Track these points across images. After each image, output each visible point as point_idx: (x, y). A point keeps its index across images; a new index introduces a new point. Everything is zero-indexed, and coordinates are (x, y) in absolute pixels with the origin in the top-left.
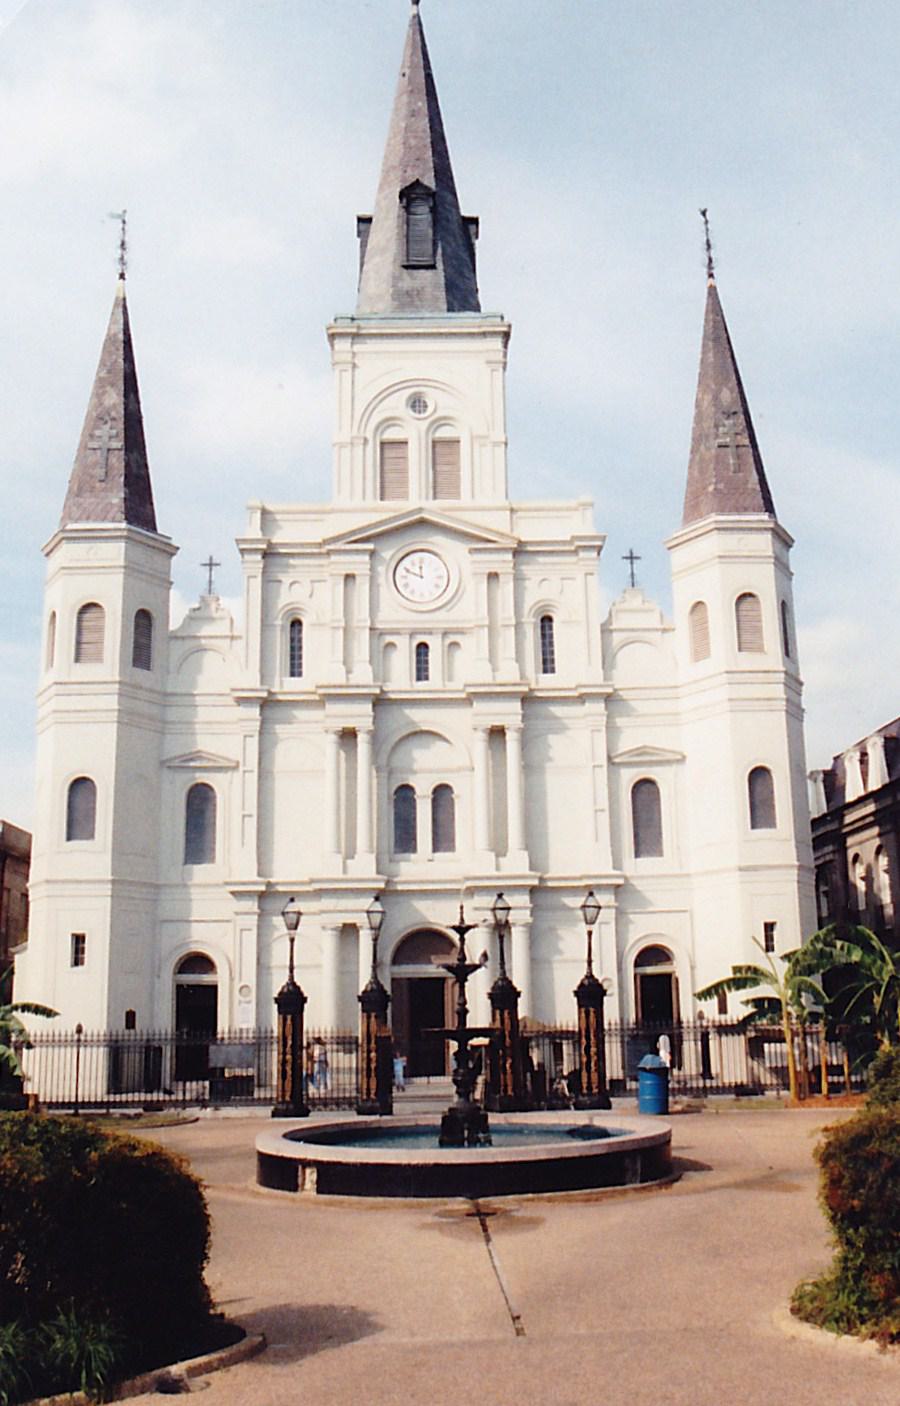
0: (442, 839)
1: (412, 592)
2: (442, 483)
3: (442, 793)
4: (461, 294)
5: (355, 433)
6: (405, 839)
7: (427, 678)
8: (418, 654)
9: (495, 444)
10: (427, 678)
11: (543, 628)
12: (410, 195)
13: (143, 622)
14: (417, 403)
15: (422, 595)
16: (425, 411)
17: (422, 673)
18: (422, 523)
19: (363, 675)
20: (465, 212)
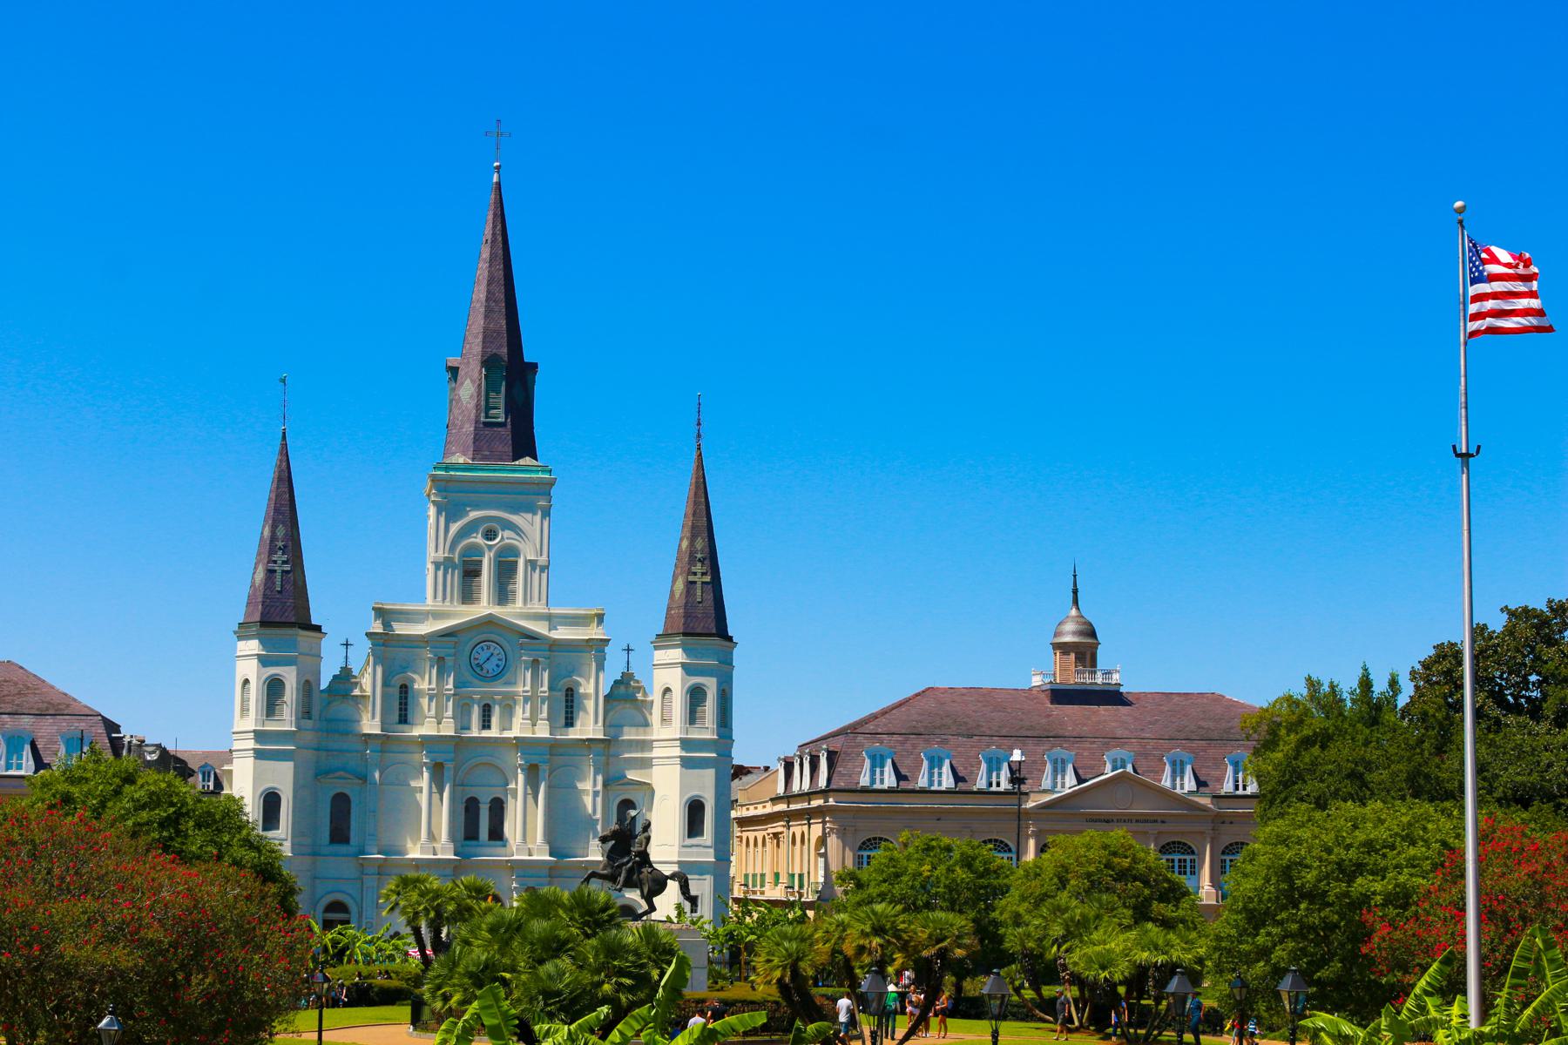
0: (497, 834)
1: (482, 670)
2: (503, 595)
3: (498, 808)
4: (524, 445)
5: (446, 555)
6: (471, 833)
7: (489, 727)
8: (484, 711)
9: (543, 569)
10: (489, 727)
11: (567, 695)
12: (489, 362)
13: (307, 688)
14: (490, 535)
15: (488, 672)
16: (494, 539)
17: (486, 725)
18: (489, 622)
19: (448, 729)
20: (527, 359)
